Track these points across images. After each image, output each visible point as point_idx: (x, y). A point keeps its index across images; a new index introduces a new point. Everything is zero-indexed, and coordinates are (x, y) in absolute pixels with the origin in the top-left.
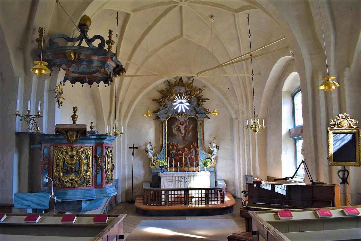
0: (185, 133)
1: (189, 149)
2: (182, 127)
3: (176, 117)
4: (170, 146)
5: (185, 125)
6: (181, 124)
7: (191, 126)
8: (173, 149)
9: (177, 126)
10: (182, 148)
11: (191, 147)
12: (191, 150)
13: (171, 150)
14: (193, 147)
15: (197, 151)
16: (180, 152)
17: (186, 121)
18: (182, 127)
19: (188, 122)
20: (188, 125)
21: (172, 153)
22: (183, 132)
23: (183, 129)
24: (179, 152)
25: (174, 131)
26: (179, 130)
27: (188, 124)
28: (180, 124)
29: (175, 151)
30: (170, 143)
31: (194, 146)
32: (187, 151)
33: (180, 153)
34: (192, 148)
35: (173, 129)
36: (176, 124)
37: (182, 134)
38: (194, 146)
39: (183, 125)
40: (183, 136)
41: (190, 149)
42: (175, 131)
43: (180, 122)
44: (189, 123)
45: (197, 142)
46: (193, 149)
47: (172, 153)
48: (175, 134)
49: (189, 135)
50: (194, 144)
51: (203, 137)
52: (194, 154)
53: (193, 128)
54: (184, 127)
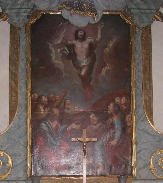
0: (91, 67)
1: (104, 116)
2: (81, 48)
3: (61, 15)
4: (41, 107)
5: (89, 40)
6: (76, 38)
7: (111, 44)
8: (50, 117)
9: (64, 44)
10: (81, 114)
11: (110, 112)
12: (110, 120)
13: (44, 120)
14: (116, 112)
15: (129, 124)
16: (74, 126)
17: (92, 27)
18: (81, 48)
19: (102, 30)
20: (101, 39)
21: (46, 129)
22: (84, 61)
23: (85, 51)
24: (69, 128)
25: (54, 58)
26: (72, 55)
27: (99, 36)
28: (72, 36)
29: (54, 124)
30: (40, 97)
31: (118, 108)
32: (95, 125)
33: (72, 129)
34: (111, 115)
35: (50, 51)
36: (62, 36)
37: (80, 69)
38: (118, 108)
39: (83, 39)
40: (83, 73)
41: (107, 118)
42: (56, 58)
43: (73, 30)
44: (102, 34)
45: (129, 96)
46: (116, 120)
47: (46, 129)
48: (59, 69)
49: (104, 71)
50: (117, 100)
51: (147, 82)
52: (118, 134)
53: (116, 49)
54: (86, 45)
